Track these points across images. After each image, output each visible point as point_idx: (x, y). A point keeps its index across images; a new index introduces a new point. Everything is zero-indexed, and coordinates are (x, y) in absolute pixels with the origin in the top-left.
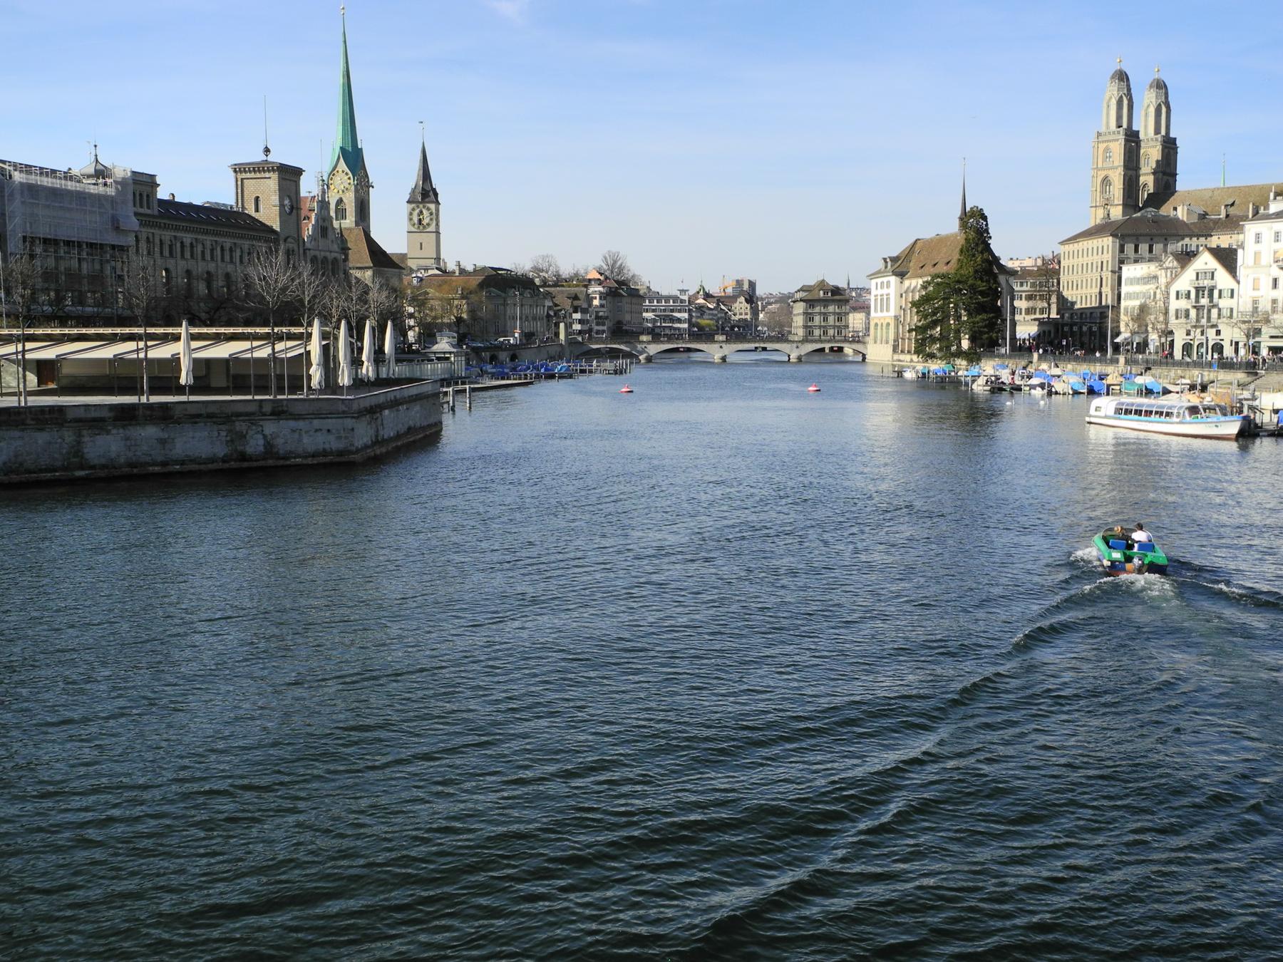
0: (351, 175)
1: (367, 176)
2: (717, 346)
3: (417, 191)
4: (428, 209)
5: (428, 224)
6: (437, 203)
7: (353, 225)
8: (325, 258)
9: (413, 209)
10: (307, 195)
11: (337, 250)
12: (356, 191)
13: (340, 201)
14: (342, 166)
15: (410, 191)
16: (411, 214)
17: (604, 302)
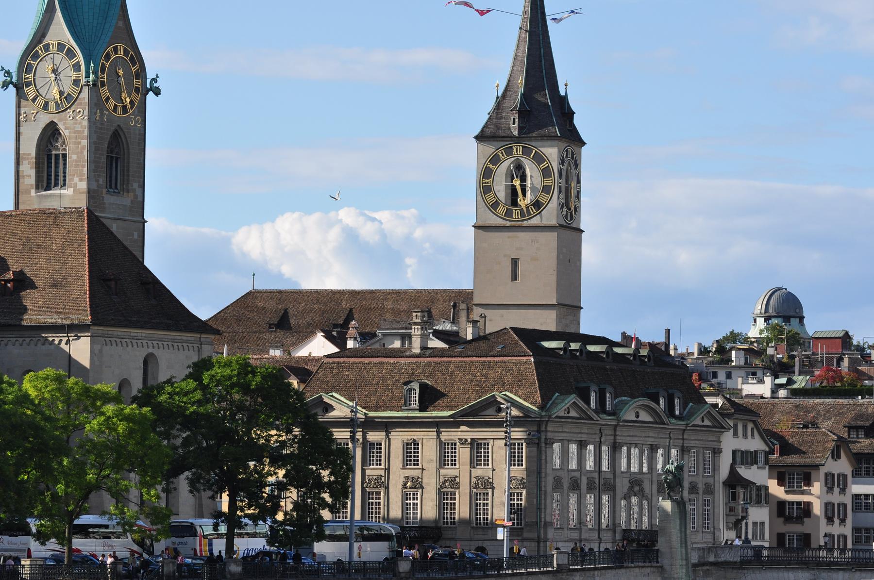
0: (80, 58)
1: (136, 58)
4: (539, 159)
5: (537, 205)
7: (82, 203)
9: (495, 160)
12: (96, 104)
13: (51, 133)
16: (487, 173)
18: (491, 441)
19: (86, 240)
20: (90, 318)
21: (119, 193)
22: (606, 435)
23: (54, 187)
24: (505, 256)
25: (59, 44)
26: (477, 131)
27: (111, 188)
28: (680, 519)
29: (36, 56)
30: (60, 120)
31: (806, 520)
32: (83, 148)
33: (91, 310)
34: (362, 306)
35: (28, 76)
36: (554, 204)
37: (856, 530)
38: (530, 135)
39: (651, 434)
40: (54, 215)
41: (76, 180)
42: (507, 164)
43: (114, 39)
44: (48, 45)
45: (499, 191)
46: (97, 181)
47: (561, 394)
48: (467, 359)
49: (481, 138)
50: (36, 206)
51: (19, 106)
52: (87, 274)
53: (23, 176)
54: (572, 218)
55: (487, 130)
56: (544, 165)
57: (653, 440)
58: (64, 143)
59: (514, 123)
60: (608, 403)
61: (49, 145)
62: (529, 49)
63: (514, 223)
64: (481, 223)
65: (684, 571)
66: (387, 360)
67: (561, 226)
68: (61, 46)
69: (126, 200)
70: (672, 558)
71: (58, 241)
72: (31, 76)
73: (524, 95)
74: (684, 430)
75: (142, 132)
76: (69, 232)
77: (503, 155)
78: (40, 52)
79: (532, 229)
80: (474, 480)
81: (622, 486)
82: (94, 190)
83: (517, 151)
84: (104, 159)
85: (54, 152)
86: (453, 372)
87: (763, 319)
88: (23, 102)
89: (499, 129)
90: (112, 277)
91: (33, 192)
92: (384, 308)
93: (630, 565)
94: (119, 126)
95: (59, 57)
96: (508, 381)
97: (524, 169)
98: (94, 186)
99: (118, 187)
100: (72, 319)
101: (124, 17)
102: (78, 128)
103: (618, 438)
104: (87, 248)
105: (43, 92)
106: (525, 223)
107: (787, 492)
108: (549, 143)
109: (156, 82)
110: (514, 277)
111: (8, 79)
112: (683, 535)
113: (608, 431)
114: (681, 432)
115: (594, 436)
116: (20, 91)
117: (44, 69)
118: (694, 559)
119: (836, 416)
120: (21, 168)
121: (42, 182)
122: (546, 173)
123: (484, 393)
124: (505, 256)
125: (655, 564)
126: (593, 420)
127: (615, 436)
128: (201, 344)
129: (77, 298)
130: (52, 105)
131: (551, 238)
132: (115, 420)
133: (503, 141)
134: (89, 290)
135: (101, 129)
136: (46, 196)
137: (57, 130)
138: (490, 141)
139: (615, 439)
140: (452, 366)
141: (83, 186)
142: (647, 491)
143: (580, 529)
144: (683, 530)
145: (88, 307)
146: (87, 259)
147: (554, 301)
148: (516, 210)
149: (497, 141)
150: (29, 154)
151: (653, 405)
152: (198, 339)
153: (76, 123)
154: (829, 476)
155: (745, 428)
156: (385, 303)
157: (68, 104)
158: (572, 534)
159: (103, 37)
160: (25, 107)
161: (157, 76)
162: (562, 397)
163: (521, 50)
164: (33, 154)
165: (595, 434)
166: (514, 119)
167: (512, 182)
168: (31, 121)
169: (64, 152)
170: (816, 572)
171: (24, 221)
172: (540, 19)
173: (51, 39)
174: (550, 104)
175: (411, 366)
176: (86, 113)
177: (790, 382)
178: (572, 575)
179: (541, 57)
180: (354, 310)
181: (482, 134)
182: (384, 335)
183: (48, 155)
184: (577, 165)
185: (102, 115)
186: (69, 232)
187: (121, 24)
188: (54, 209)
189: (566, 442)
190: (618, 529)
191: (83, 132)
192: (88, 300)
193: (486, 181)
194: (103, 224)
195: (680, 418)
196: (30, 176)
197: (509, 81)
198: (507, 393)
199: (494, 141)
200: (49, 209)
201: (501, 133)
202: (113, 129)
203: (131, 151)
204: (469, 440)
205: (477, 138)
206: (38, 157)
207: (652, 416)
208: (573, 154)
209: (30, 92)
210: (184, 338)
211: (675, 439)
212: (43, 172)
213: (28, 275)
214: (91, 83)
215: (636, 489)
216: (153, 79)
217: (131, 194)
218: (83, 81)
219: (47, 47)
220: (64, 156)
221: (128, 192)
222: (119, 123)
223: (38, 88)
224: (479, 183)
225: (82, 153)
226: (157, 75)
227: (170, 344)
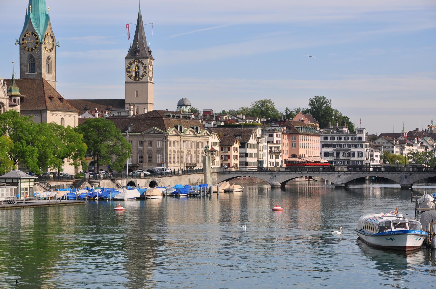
2: (336, 175)
4: (143, 64)
9: (131, 64)
16: (129, 68)
17: (279, 139)
26: (125, 56)
30: (33, 53)
41: (38, 70)
49: (126, 58)
56: (144, 66)
60: (182, 130)
64: (127, 81)
65: (210, 174)
102: (38, 56)
106: (139, 81)
118: (212, 171)
130: (30, 50)
142: (192, 153)
151: (193, 130)
155: (214, 136)
190: (185, 164)
195: (199, 133)
205: (125, 58)
212: (28, 68)
215: (189, 153)
217: (52, 74)
220: (34, 64)
224: (126, 70)
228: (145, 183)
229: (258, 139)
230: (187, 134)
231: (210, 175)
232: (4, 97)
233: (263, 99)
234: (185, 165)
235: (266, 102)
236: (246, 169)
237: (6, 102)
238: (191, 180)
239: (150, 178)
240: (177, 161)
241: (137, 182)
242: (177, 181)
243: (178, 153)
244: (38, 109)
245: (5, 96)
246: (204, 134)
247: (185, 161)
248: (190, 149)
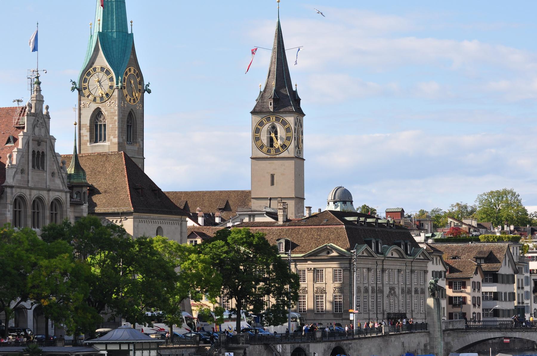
0: (113, 74)
1: (139, 74)
3: (267, 95)
4: (284, 123)
5: (284, 146)
6: (300, 113)
7: (116, 149)
8: (40, 199)
9: (261, 124)
10: (15, 105)
11: (61, 187)
12: (122, 98)
13: (97, 113)
14: (102, 61)
15: (257, 95)
16: (257, 131)
18: (324, 269)
19: (125, 169)
20: (133, 208)
21: (132, 144)
22: (379, 265)
23: (99, 141)
24: (267, 173)
25: (101, 68)
26: (251, 109)
27: (128, 141)
28: (437, 307)
29: (89, 74)
30: (103, 107)
31: (464, 305)
32: (115, 121)
33: (132, 205)
34: (192, 199)
35: (85, 84)
36: (292, 147)
37: (483, 310)
38: (279, 111)
39: (399, 264)
40: (105, 156)
41: (112, 137)
42: (267, 127)
43: (130, 65)
44: (95, 68)
45: (264, 140)
46: (122, 138)
47: (359, 244)
48: (309, 227)
49: (254, 112)
50: (90, 152)
51: (80, 100)
52: (128, 186)
53: (83, 136)
54: (300, 153)
55: (257, 109)
56: (286, 127)
57: (399, 266)
58: (104, 118)
59: (271, 105)
60: (380, 248)
61: (96, 120)
62: (277, 67)
63: (271, 156)
64: (254, 156)
66: (265, 228)
67: (296, 157)
68: (102, 69)
69: (135, 147)
70: (434, 327)
71: (110, 169)
72: (86, 84)
73: (275, 91)
74: (412, 261)
75: (142, 112)
76: (115, 164)
77: (265, 121)
78: (91, 72)
79: (286, 159)
80: (315, 289)
81: (386, 290)
82: (121, 142)
83: (272, 119)
84: (125, 127)
85: (99, 123)
86: (302, 234)
87: (333, 203)
88: (82, 98)
89: (263, 108)
90: (140, 187)
91: (88, 144)
92: (204, 200)
93: (415, 331)
94: (132, 109)
95: (102, 75)
96: (332, 238)
97: (276, 129)
98: (121, 141)
99: (131, 141)
100: (123, 210)
101: (133, 53)
102: (112, 110)
103: (384, 266)
104: (126, 172)
105: (92, 92)
106: (277, 156)
107: (453, 292)
108: (289, 115)
109: (149, 86)
110: (272, 183)
111: (75, 86)
112: (439, 315)
113: (380, 263)
114: (381, 261)
115: (373, 266)
116: (81, 92)
117: (93, 80)
118: (444, 328)
119: (468, 252)
120: (82, 132)
121: (93, 138)
122: (288, 130)
123: (320, 244)
124: (267, 173)
125: (426, 331)
126: (374, 257)
127: (383, 265)
128: (182, 221)
129: (124, 199)
130: (98, 100)
131: (292, 162)
132: (197, 262)
133: (265, 114)
134: (130, 194)
135: (124, 111)
136: (95, 146)
137: (101, 112)
138: (258, 114)
139: (383, 267)
140: (301, 231)
141: (116, 140)
142: (397, 293)
143: (369, 313)
144: (439, 313)
145: (131, 203)
146: (127, 178)
147: (293, 196)
148: (272, 149)
149: (262, 114)
150: (86, 124)
151: (399, 248)
152: (180, 219)
153: (111, 108)
154: (474, 283)
155: (436, 259)
156: (204, 198)
157: (107, 98)
158: (366, 316)
159: (124, 64)
160: (83, 100)
161: (149, 84)
162: (360, 246)
163: (273, 67)
164: (88, 125)
165: (374, 264)
166: (271, 103)
167: (270, 135)
168: (86, 107)
169: (104, 123)
170: (505, 332)
171: (90, 159)
172: (282, 52)
173: (97, 65)
174: (289, 95)
175: (279, 231)
176: (117, 102)
177: (433, 235)
178: (390, 337)
179: (283, 71)
180: (188, 202)
181: (254, 111)
182: (240, 215)
183: (95, 125)
184: (301, 126)
185: (124, 104)
186: (115, 164)
187: (132, 57)
188: (105, 153)
189: (362, 269)
190: (385, 313)
191: (115, 113)
192: (130, 199)
193: (257, 134)
194: (132, 160)
195: (410, 255)
196: (86, 136)
197: (267, 83)
198: (332, 244)
199: (260, 114)
200: (103, 153)
201: (264, 110)
202: (129, 111)
203: (137, 122)
204: (313, 269)
205: (251, 113)
206: (90, 126)
207: (398, 254)
208: (300, 120)
209: (86, 92)
210: (174, 218)
211: (408, 266)
213: (96, 187)
214: (120, 87)
216: (147, 85)
217: (138, 144)
218: (115, 86)
219: (95, 69)
220: (105, 125)
221: (136, 143)
222: (132, 108)
223: (90, 90)
225: (115, 123)
226: (149, 83)
227: (168, 221)
228: (325, 350)
229: (515, 265)
230: (388, 256)
231: (441, 336)
232: (62, 188)
233: (500, 188)
234: (385, 317)
235: (506, 193)
236: (495, 323)
237: (66, 198)
238: (406, 345)
239: (332, 341)
240: (370, 308)
241: (309, 349)
242: (381, 346)
243: (372, 292)
244: (116, 211)
245: (64, 187)
246: (418, 257)
247: (385, 309)
248: (394, 286)
